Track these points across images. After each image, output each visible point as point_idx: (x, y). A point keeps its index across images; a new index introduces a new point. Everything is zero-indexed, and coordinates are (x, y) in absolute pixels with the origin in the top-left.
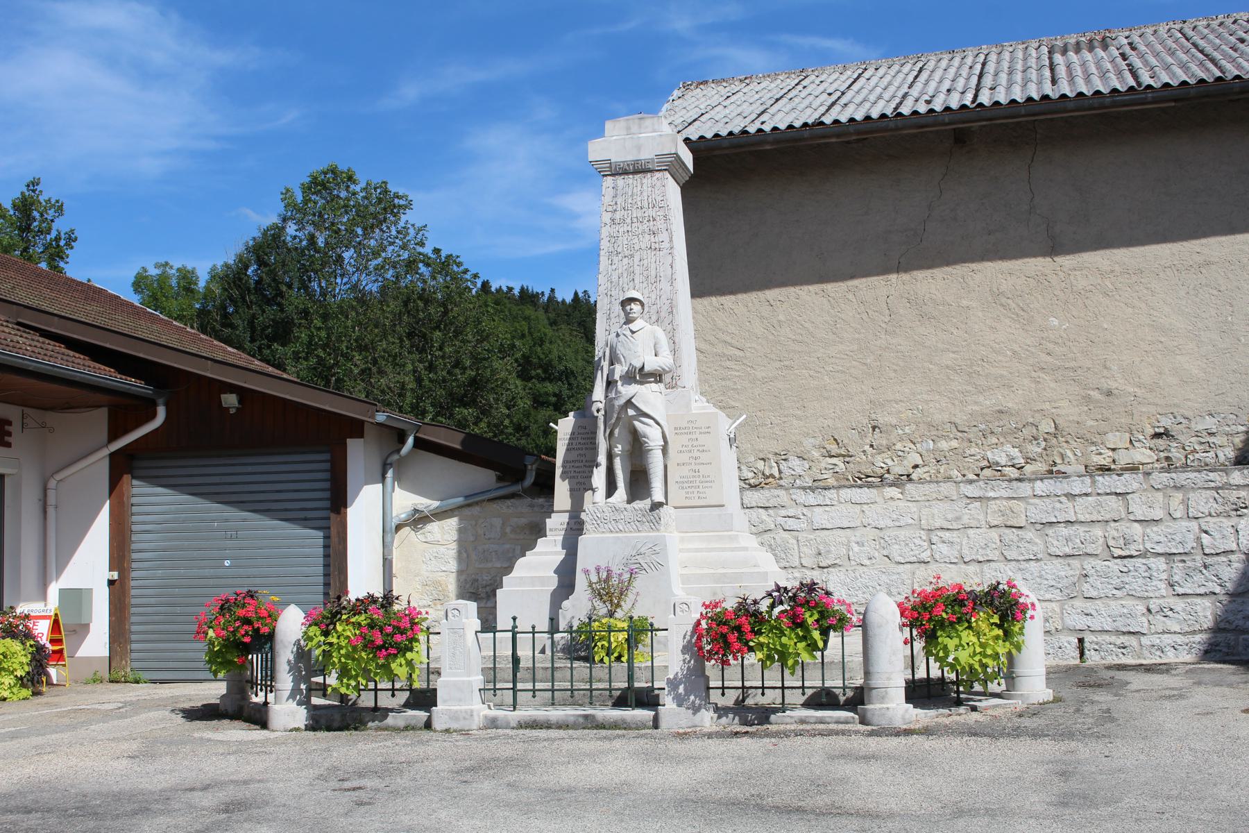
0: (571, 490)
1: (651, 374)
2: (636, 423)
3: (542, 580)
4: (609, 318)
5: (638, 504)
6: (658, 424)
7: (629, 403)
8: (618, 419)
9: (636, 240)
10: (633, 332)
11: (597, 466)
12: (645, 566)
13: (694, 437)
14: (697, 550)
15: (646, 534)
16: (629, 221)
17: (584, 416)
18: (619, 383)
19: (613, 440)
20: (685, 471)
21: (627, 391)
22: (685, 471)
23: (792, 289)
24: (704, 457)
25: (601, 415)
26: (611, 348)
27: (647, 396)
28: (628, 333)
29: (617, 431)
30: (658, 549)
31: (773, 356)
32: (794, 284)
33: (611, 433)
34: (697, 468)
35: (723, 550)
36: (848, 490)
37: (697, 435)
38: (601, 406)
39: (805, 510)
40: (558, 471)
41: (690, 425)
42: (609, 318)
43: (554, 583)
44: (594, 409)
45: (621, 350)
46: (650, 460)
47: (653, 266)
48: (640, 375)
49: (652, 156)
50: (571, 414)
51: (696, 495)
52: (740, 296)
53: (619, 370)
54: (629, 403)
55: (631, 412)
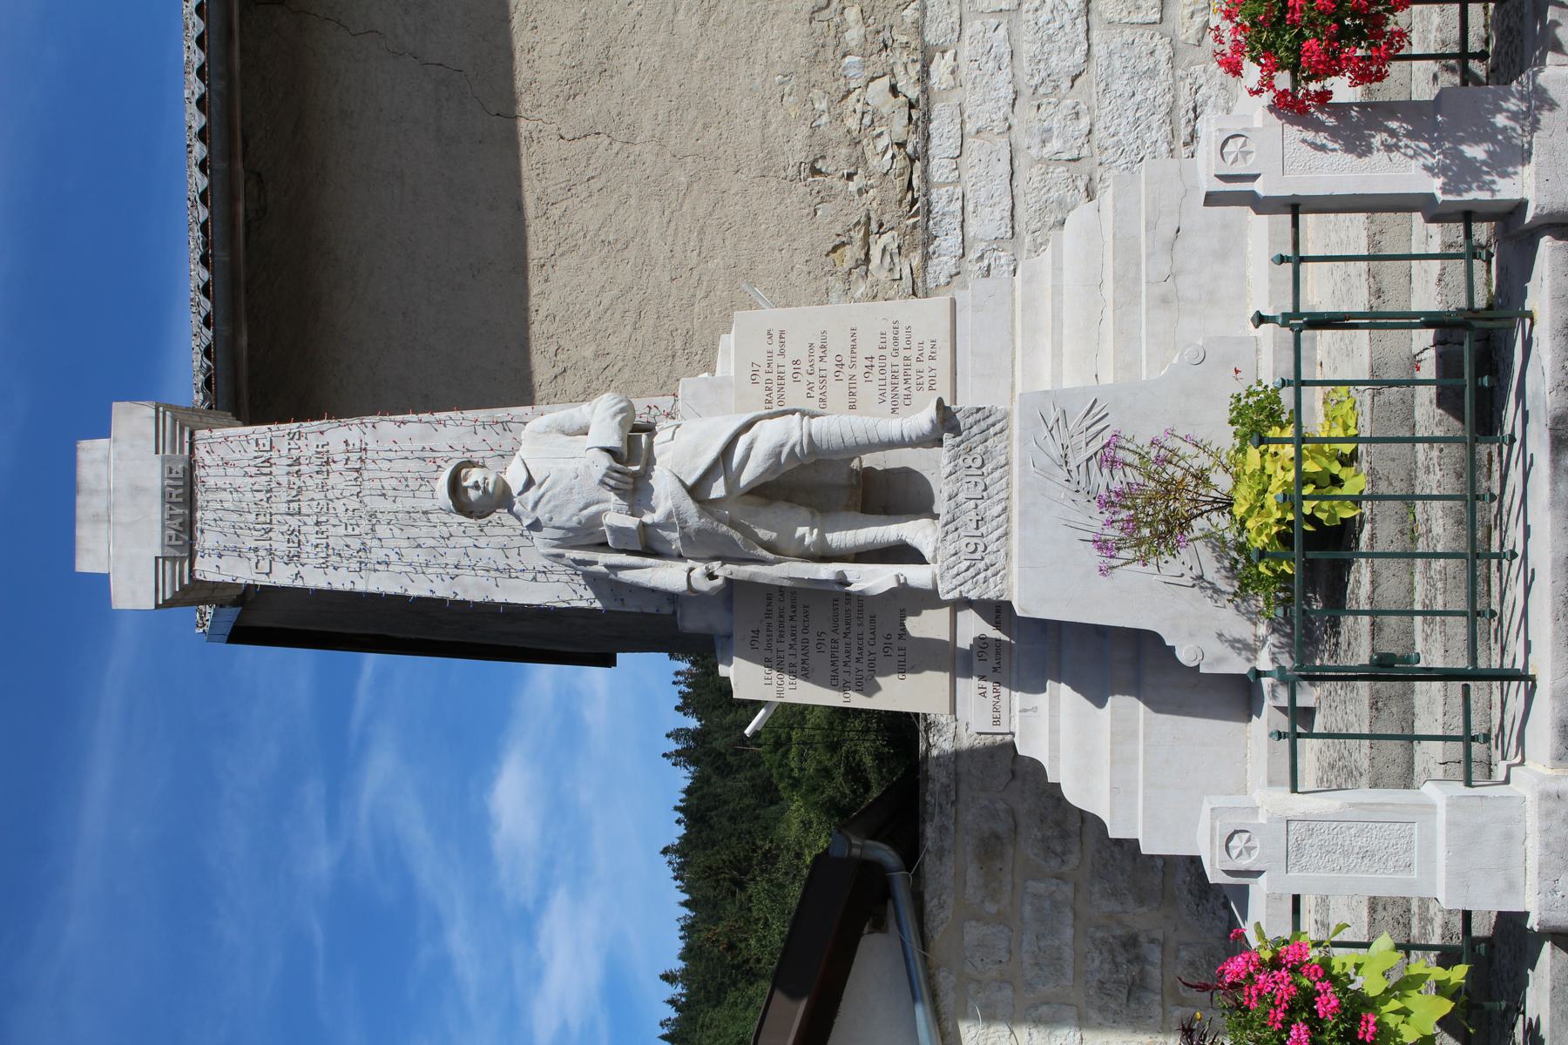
0: (903, 669)
1: (632, 442)
2: (746, 478)
3: (1122, 735)
4: (508, 571)
5: (941, 490)
6: (748, 426)
7: (696, 491)
8: (733, 524)
9: (339, 505)
10: (529, 483)
11: (842, 581)
12: (1096, 445)
13: (789, 369)
14: (1057, 354)
15: (1016, 446)
16: (294, 522)
17: (729, 637)
18: (648, 518)
20: (868, 391)
21: (666, 495)
22: (868, 391)
23: (535, 329)
25: (723, 571)
26: (565, 543)
27: (680, 454)
28: (532, 494)
29: (764, 534)
30: (1052, 416)
31: (664, 370)
32: (525, 324)
33: (769, 546)
34: (861, 363)
35: (1057, 291)
36: (934, 163)
38: (700, 568)
39: (972, 255)
40: (857, 701)
41: (762, 377)
42: (508, 571)
43: (1127, 708)
44: (704, 585)
45: (569, 516)
46: (836, 442)
47: (398, 465)
48: (630, 464)
49: (157, 460)
50: (723, 670)
51: (926, 365)
53: (616, 516)
54: (696, 491)
55: (718, 490)
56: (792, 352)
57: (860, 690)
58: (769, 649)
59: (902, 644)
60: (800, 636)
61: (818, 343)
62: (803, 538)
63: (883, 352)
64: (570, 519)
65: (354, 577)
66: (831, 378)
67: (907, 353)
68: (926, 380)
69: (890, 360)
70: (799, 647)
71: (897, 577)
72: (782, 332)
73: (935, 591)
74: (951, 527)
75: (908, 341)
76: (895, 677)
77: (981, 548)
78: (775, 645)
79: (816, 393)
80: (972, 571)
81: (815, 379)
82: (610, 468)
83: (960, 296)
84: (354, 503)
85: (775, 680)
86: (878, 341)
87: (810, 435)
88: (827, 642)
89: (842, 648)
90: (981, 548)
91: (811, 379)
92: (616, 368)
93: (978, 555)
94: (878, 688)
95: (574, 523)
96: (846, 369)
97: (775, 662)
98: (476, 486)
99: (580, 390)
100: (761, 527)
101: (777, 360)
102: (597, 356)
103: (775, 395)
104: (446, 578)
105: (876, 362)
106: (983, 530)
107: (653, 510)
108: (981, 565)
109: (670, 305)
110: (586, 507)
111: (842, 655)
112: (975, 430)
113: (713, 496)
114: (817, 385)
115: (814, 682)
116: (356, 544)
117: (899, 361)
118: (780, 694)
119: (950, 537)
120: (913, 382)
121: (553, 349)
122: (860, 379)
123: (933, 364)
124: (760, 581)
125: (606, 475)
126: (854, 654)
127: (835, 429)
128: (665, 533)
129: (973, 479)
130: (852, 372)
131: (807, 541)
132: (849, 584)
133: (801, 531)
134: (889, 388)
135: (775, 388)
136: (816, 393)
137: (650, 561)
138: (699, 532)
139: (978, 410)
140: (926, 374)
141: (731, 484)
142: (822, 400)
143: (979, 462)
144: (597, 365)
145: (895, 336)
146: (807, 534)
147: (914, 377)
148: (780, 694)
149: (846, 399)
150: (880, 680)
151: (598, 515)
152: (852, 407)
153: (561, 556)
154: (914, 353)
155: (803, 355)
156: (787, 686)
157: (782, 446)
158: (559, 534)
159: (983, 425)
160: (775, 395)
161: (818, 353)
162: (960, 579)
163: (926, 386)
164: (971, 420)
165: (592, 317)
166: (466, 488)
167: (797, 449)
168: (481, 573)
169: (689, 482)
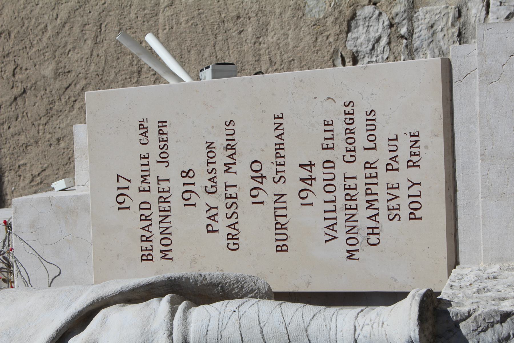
13: (177, 186)
20: (307, 221)
22: (307, 221)
34: (294, 174)
37: (173, 173)
41: (136, 198)
51: (403, 176)
56: (178, 161)
61: (220, 142)
63: (328, 155)
66: (244, 199)
68: (404, 201)
69: (341, 168)
72: (162, 124)
75: (371, 137)
79: (222, 224)
81: (218, 201)
83: (462, 56)
91: (212, 200)
92: (79, 87)
99: (42, 112)
101: (157, 170)
102: (57, 75)
103: (155, 229)
105: (318, 172)
109: (133, 16)
114: (222, 211)
117: (357, 169)
120: (382, 205)
121: (10, 68)
122: (293, 201)
123: (414, 174)
130: (279, 188)
134: (341, 216)
135: (156, 218)
136: (222, 224)
140: (403, 193)
142: (231, 237)
145: (350, 126)
147: (383, 197)
149: (270, 236)
152: (282, 248)
154: (382, 156)
155: (198, 162)
160: (155, 229)
161: (222, 157)
163: (405, 212)
165: (49, 33)
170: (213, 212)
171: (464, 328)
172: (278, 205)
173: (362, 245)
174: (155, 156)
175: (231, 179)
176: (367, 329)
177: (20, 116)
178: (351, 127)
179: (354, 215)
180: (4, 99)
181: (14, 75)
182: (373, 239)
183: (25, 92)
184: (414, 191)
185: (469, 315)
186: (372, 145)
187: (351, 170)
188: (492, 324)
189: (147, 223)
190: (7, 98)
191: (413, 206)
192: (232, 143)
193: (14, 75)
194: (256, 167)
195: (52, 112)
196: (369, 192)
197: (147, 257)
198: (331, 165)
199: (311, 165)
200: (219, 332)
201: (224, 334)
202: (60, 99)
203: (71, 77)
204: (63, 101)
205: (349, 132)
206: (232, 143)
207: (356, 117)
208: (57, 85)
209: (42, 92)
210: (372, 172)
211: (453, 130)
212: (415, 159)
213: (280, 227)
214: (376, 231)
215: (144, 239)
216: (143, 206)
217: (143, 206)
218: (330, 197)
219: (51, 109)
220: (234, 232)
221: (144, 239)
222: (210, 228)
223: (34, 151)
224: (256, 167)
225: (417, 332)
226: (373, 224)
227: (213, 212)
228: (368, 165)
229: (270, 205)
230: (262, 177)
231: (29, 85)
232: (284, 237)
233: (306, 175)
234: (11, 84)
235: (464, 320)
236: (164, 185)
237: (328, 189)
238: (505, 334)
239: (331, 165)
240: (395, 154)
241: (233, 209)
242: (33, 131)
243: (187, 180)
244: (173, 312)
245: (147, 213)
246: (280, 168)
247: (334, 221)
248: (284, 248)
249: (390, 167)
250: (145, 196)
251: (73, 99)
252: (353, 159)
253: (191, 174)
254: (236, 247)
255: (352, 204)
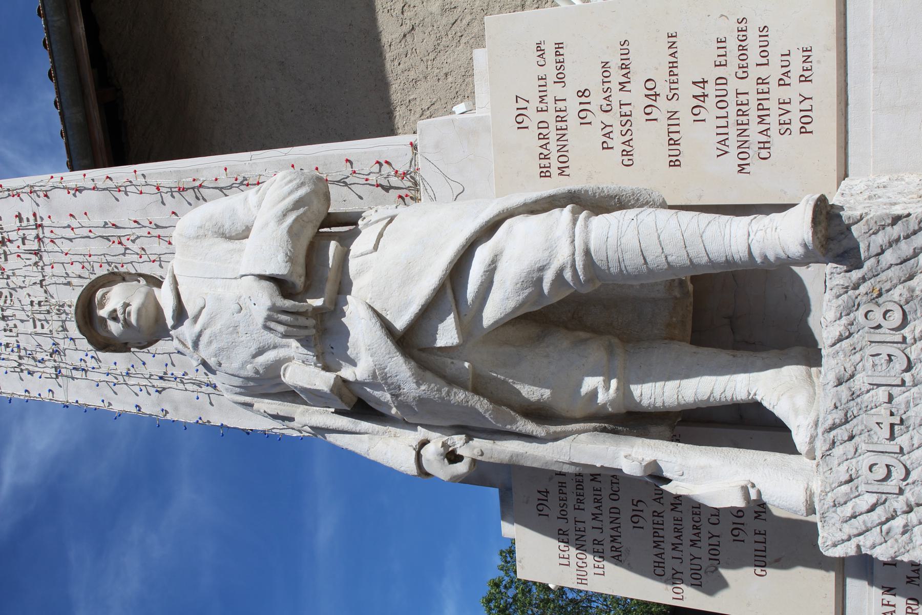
2: (491, 314)
5: (825, 321)
6: (490, 229)
7: (410, 341)
8: (479, 386)
9: (22, 294)
10: (180, 314)
13: (573, 105)
18: (347, 373)
19: (563, 406)
20: (699, 137)
22: (699, 137)
24: (649, 63)
29: (531, 392)
33: (539, 413)
34: (687, 91)
37: (569, 93)
38: (436, 441)
41: (533, 118)
46: (632, 262)
52: (396, 96)
54: (410, 341)
55: (447, 334)
56: (574, 82)
57: (697, 585)
58: (563, 517)
59: (759, 525)
60: (607, 504)
61: (615, 62)
62: (594, 394)
63: (721, 72)
64: (243, 366)
65: (52, 384)
66: (638, 116)
67: (763, 72)
68: (795, 116)
69: (734, 85)
70: (606, 517)
71: (745, 490)
72: (559, 46)
73: (811, 530)
74: (841, 433)
75: (764, 53)
76: (748, 572)
77: (898, 473)
78: (571, 514)
79: (617, 141)
80: (880, 513)
81: (613, 119)
82: (273, 309)
84: (38, 294)
85: (573, 560)
86: (713, 53)
87: (587, 253)
88: (647, 514)
89: (669, 524)
90: (898, 473)
92: (465, 22)
93: (892, 486)
94: (723, 584)
95: (249, 371)
96: (661, 102)
97: (572, 536)
98: (114, 316)
99: (431, 48)
100: (523, 381)
101: (554, 90)
102: (444, 11)
103: (553, 146)
104: (152, 390)
105: (710, 89)
106: (903, 440)
107: (353, 363)
108: (899, 504)
110: (260, 352)
111: (669, 536)
112: (889, 257)
113: (441, 342)
114: (617, 128)
115: (630, 568)
116: (47, 344)
117: (749, 86)
118: (582, 579)
119: (838, 451)
120: (773, 120)
122: (685, 117)
123: (806, 89)
124: (528, 464)
125: (269, 318)
126: (688, 534)
127: (630, 241)
128: (377, 394)
129: (885, 350)
130: (673, 105)
131: (602, 398)
132: (668, 481)
133: (590, 383)
134: (733, 131)
135: (553, 136)
136: (617, 141)
137: (364, 425)
138: (421, 401)
139: (896, 219)
140: (795, 108)
141: (469, 324)
142: (625, 153)
143: (896, 318)
144: (445, 21)
146: (600, 388)
147: (775, 112)
148: (582, 579)
149: (664, 151)
150: (727, 574)
151: (278, 364)
153: (250, 405)
154: (774, 72)
156: (590, 570)
157: (542, 269)
158: (238, 382)
159: (905, 248)
160: (553, 146)
161: (616, 76)
162: (858, 524)
163: (796, 126)
164: (880, 239)
166: (103, 320)
167: (568, 275)
168: (190, 387)
169: (400, 324)
170: (608, 130)
171: (856, 231)
172: (671, 122)
173: (754, 160)
174: (552, 76)
175: (625, 97)
176: (760, 234)
177: (409, 52)
178: (743, 44)
179: (745, 130)
180: (393, 37)
181: (402, 13)
182: (764, 153)
183: (413, 28)
184: (806, 105)
185: (861, 219)
186: (764, 61)
187: (743, 86)
188: (883, 227)
189: (545, 141)
190: (397, 35)
191: (804, 120)
192: (627, 62)
193: (402, 13)
194: (650, 85)
195: (439, 48)
196: (761, 107)
197: (545, 174)
198: (724, 81)
199: (704, 82)
200: (619, 239)
201: (623, 240)
202: (447, 35)
203: (456, 14)
204: (450, 36)
205: (742, 48)
206: (627, 62)
207: (748, 33)
208: (444, 22)
209: (430, 29)
210: (764, 87)
211: (845, 45)
212: (807, 74)
213: (673, 143)
214: (767, 145)
215: (542, 156)
216: (540, 125)
217: (540, 125)
218: (722, 113)
219: (438, 44)
220: (628, 149)
221: (542, 156)
222: (605, 146)
223: (423, 86)
224: (650, 85)
225: (810, 234)
226: (764, 139)
227: (608, 130)
228: (760, 81)
229: (663, 122)
230: (656, 95)
231: (417, 22)
232: (677, 153)
233: (699, 92)
234: (400, 21)
235: (856, 223)
236: (561, 105)
237: (721, 105)
238: (895, 236)
239: (724, 81)
240: (786, 69)
241: (627, 127)
242: (422, 67)
243: (583, 100)
244: (575, 221)
245: (544, 131)
246: (673, 86)
247: (726, 137)
248: (677, 163)
249: (782, 82)
250: (543, 116)
251: (459, 34)
252: (745, 75)
253: (587, 93)
254: (631, 162)
255: (744, 119)
